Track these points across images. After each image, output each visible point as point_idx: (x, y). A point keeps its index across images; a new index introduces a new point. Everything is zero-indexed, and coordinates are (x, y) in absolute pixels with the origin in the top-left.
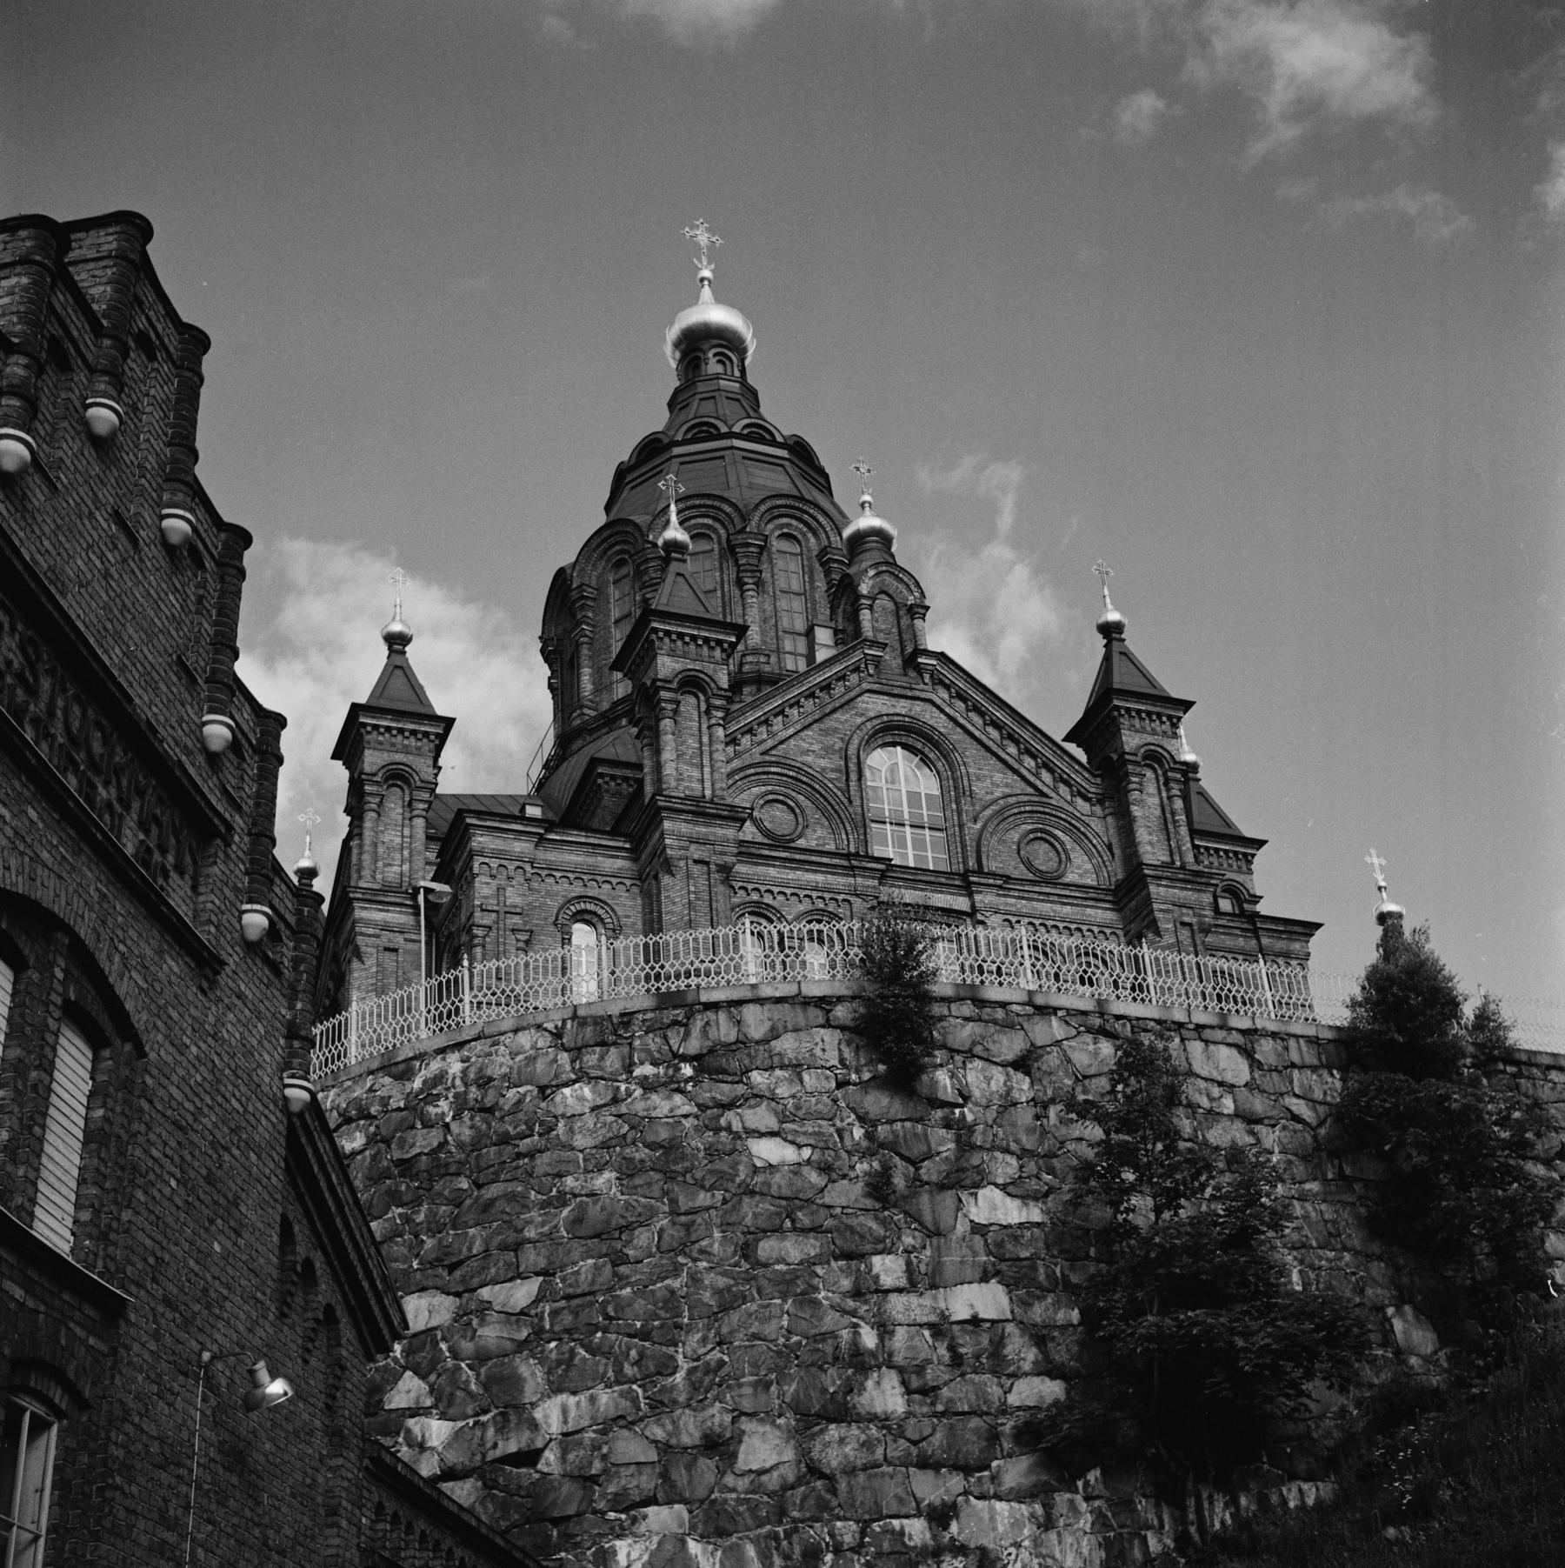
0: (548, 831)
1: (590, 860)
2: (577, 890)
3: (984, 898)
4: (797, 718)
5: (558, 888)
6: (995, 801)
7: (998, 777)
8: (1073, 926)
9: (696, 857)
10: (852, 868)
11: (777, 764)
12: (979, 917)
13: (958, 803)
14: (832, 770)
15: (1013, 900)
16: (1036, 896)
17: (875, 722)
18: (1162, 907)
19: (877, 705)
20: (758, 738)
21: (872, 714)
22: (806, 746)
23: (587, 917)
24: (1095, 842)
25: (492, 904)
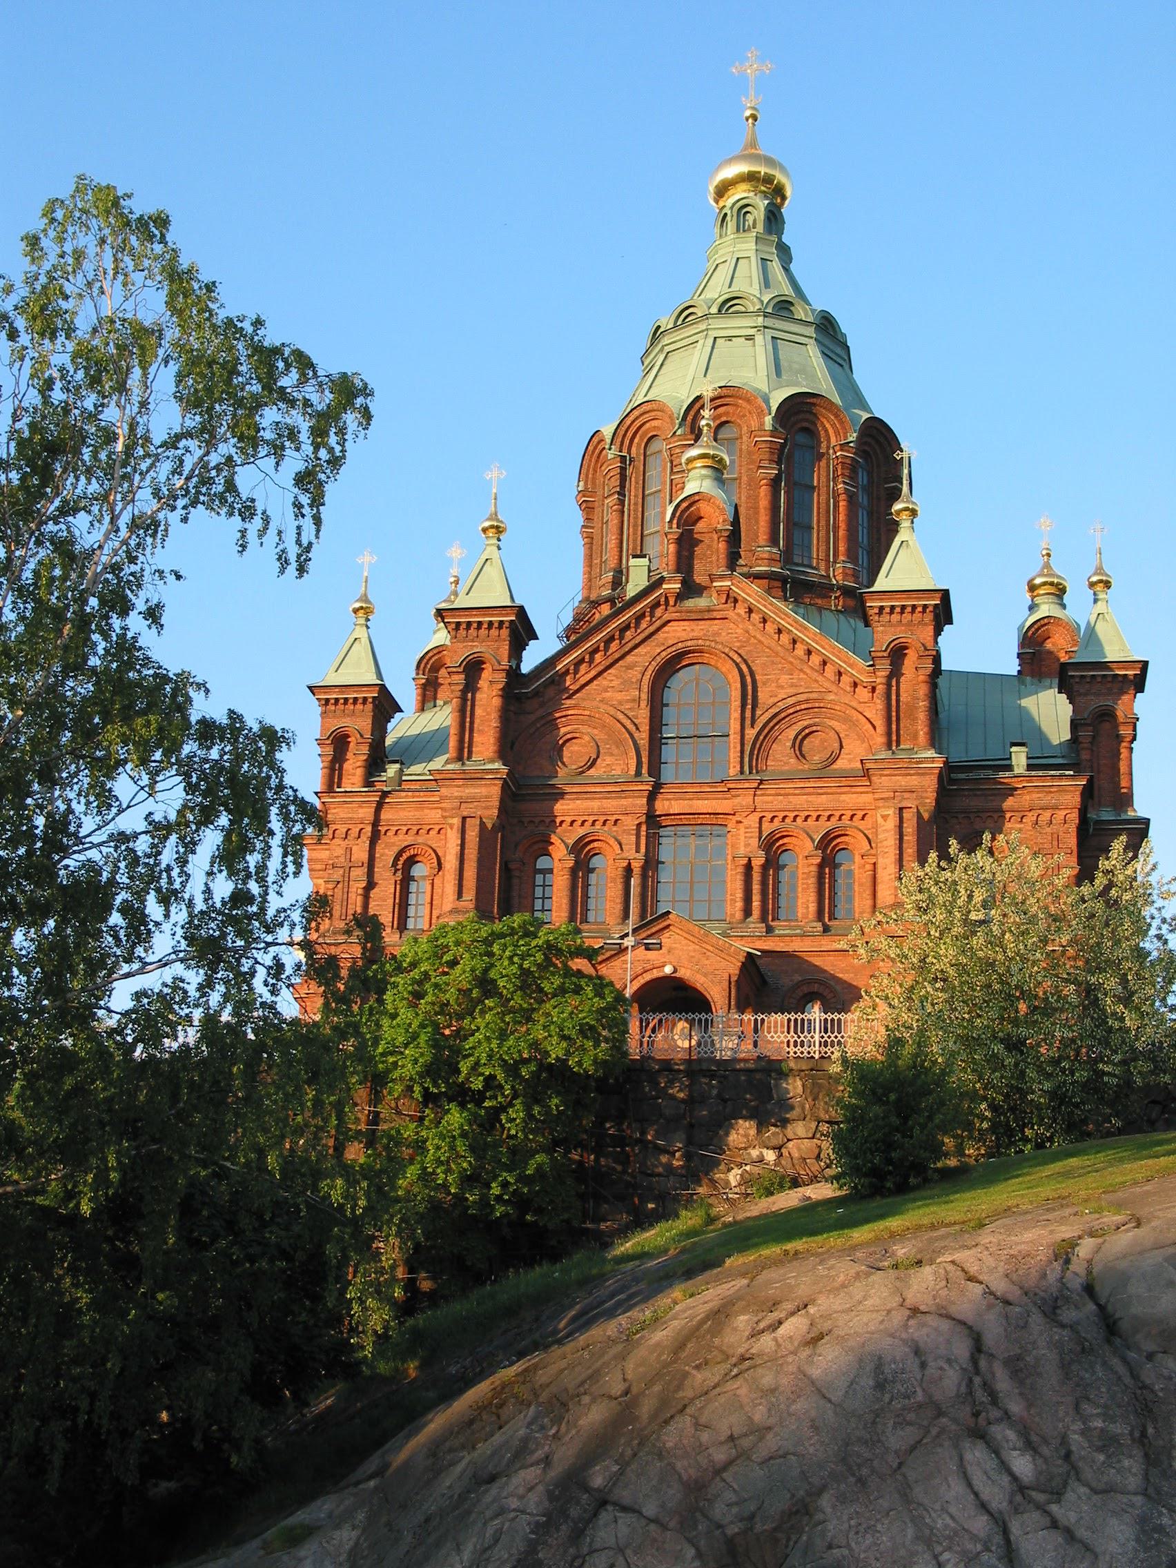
1: (418, 814)
2: (409, 840)
9: (465, 814)
14: (628, 701)
16: (791, 791)
17: (669, 650)
21: (671, 643)
22: (605, 683)
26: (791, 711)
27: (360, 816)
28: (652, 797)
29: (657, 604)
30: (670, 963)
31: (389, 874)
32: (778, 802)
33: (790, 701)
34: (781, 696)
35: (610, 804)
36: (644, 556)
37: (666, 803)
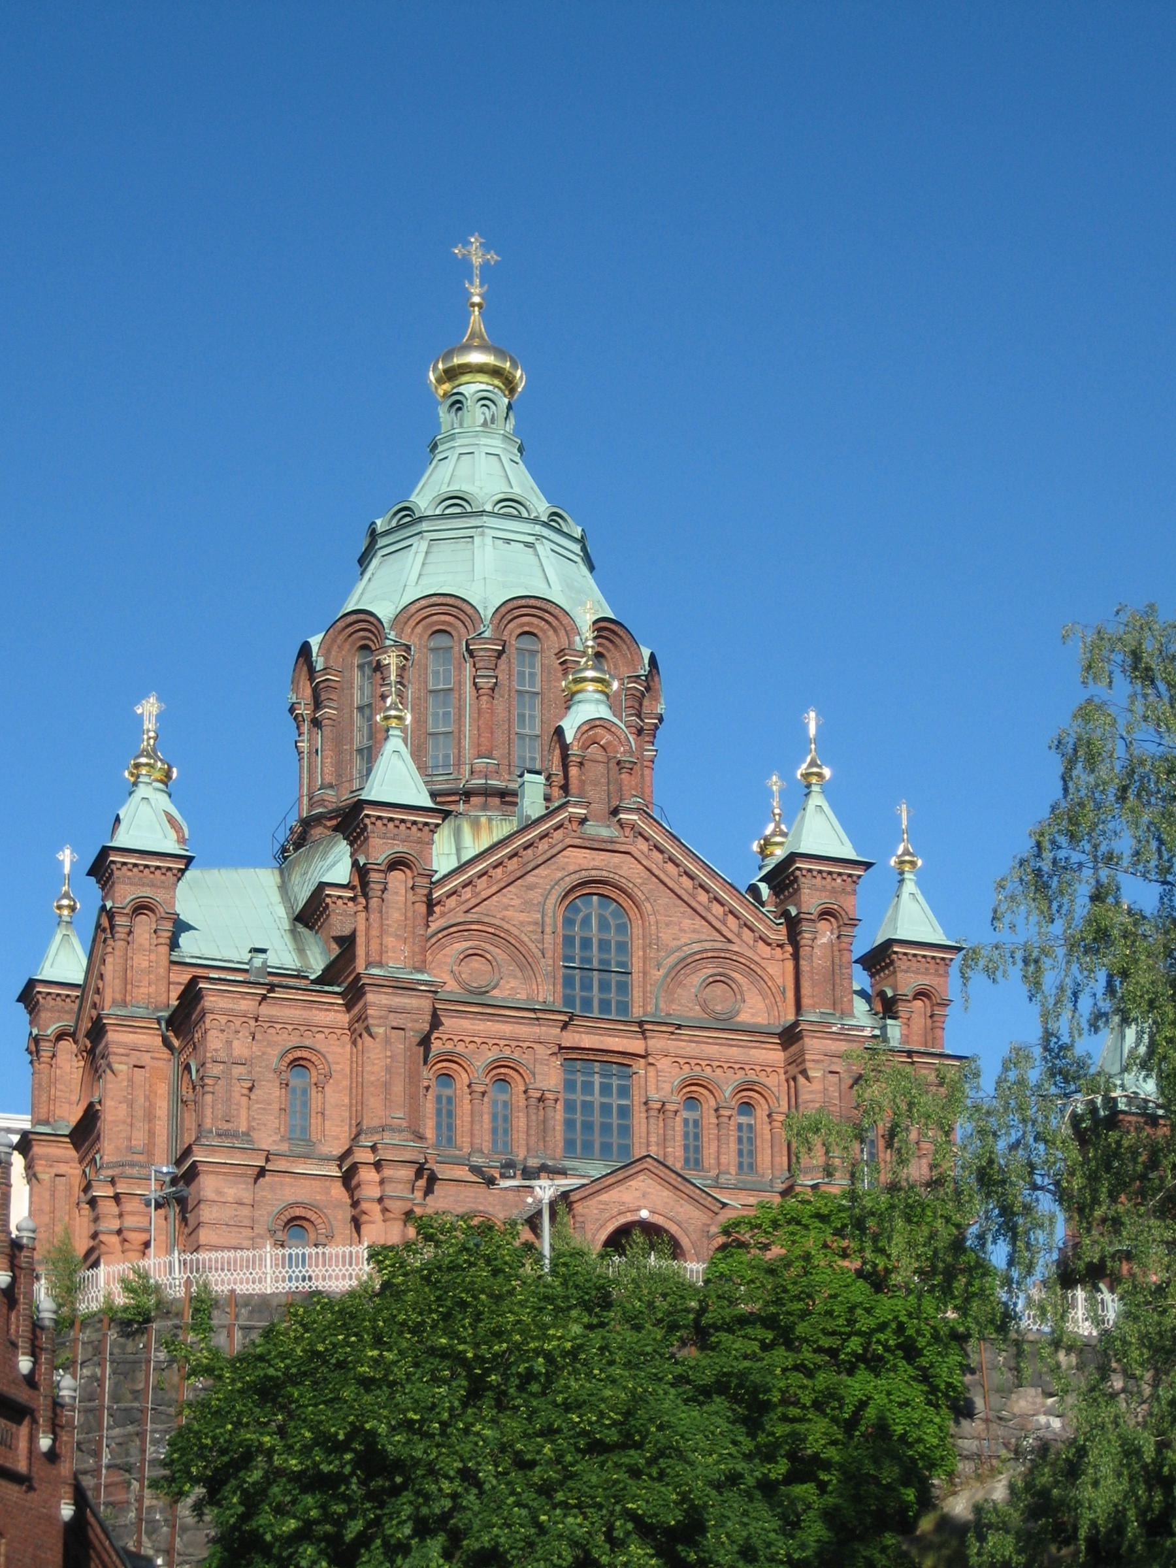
0: (270, 991)
2: (295, 1040)
3: (656, 1043)
4: (500, 877)
5: (279, 1038)
6: (679, 949)
7: (687, 923)
8: (737, 1066)
10: (538, 1019)
11: (478, 922)
12: (651, 1060)
13: (644, 952)
14: (529, 923)
15: (684, 1044)
17: (577, 876)
18: (813, 1057)
19: (580, 861)
20: (464, 898)
21: (572, 868)
22: (505, 900)
23: (302, 1062)
24: (770, 984)
25: (222, 1055)
26: (698, 957)
27: (243, 1008)
28: (565, 1026)
29: (559, 826)
30: (645, 1207)
31: (272, 1075)
32: (691, 1049)
33: (696, 947)
34: (683, 941)
35: (523, 1030)
36: (538, 773)
37: (577, 1036)
